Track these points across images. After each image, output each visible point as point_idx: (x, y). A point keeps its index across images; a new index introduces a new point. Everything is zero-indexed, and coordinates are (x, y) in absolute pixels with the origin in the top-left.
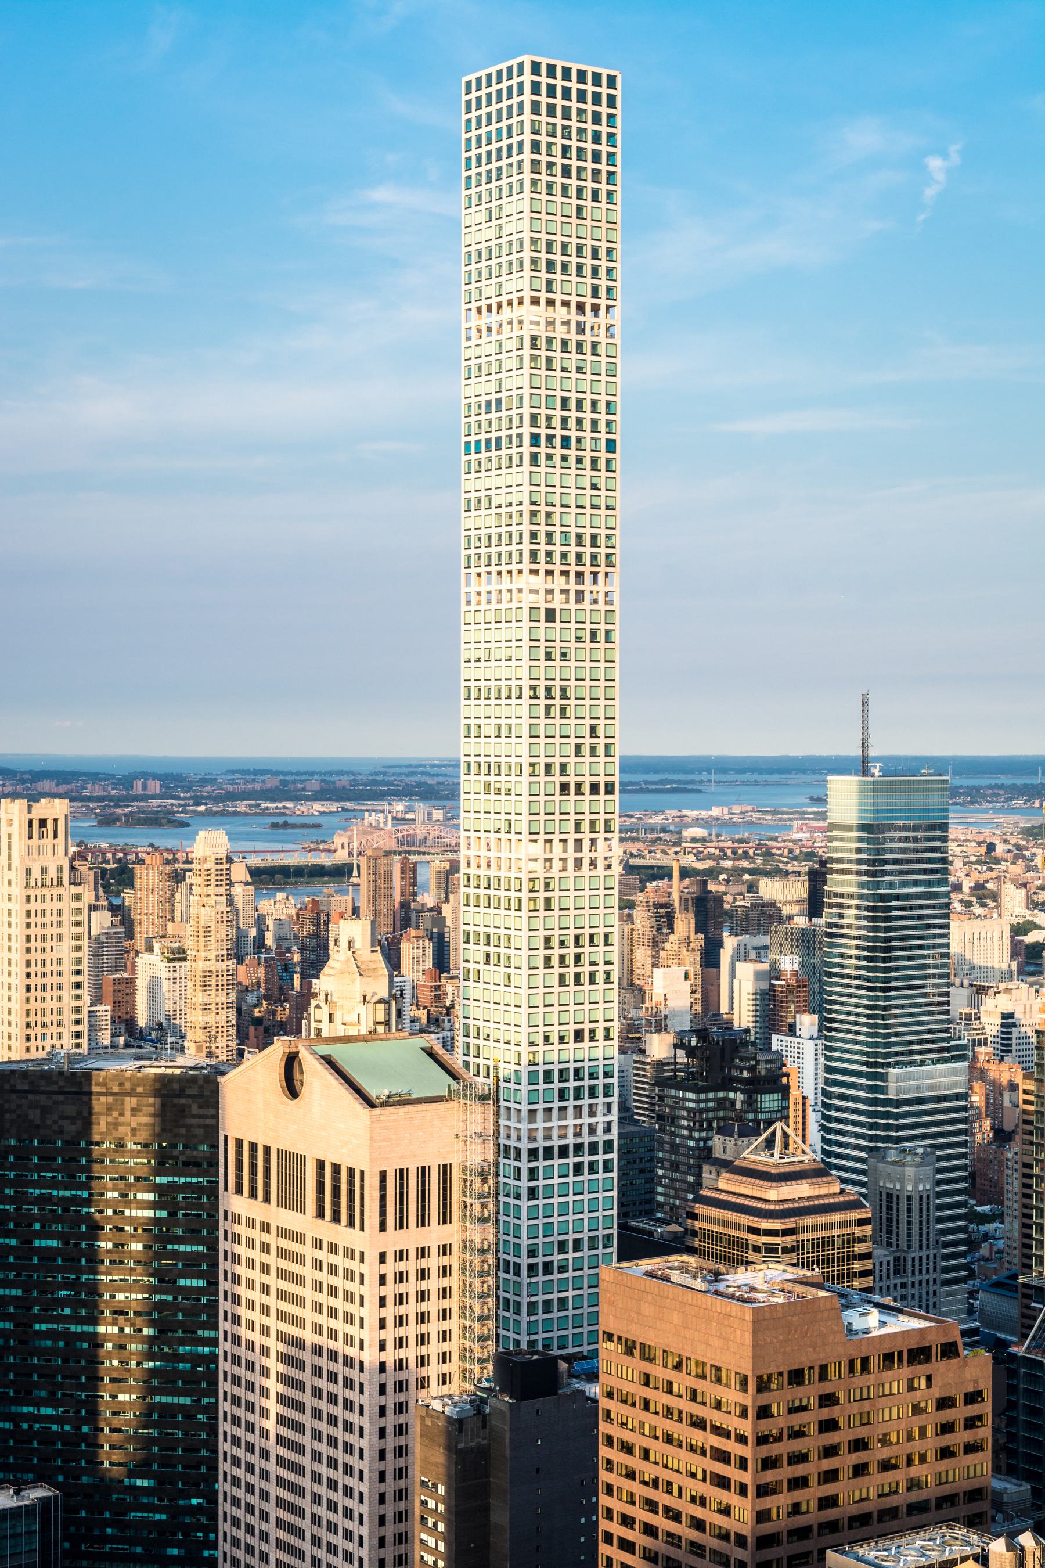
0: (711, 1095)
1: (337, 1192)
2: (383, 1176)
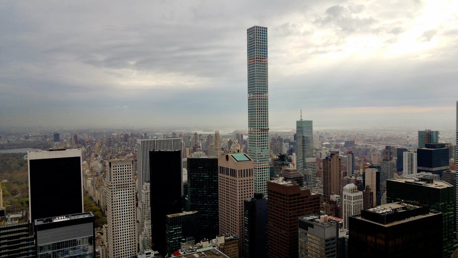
1: (233, 173)
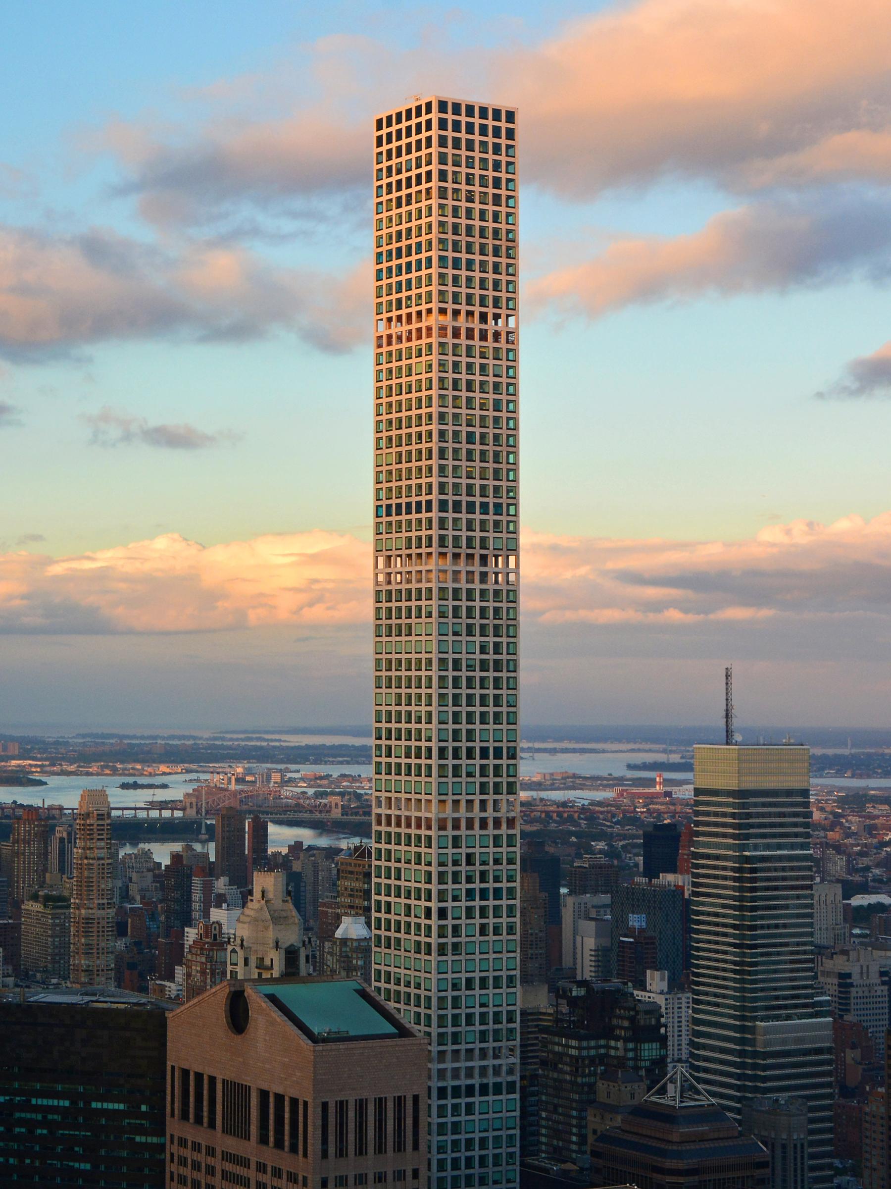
0: (593, 1043)
1: (279, 1119)
2: (325, 1106)
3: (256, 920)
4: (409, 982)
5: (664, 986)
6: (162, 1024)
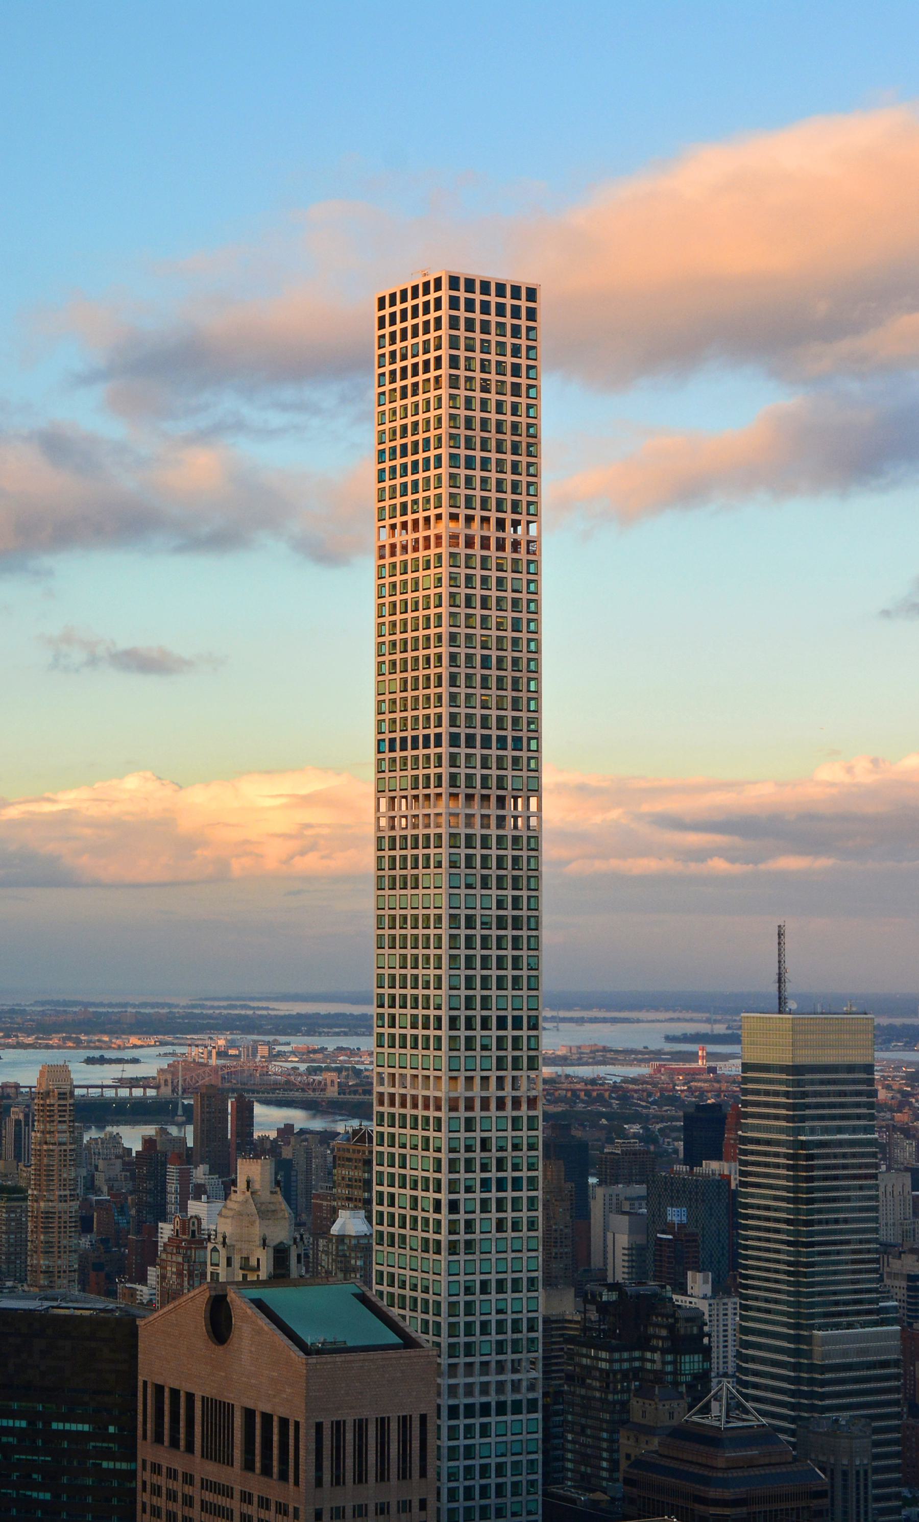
0: (626, 1355)
1: (267, 1443)
2: (319, 1427)
3: (240, 1214)
4: (416, 1286)
5: (708, 1289)
6: (133, 1333)
